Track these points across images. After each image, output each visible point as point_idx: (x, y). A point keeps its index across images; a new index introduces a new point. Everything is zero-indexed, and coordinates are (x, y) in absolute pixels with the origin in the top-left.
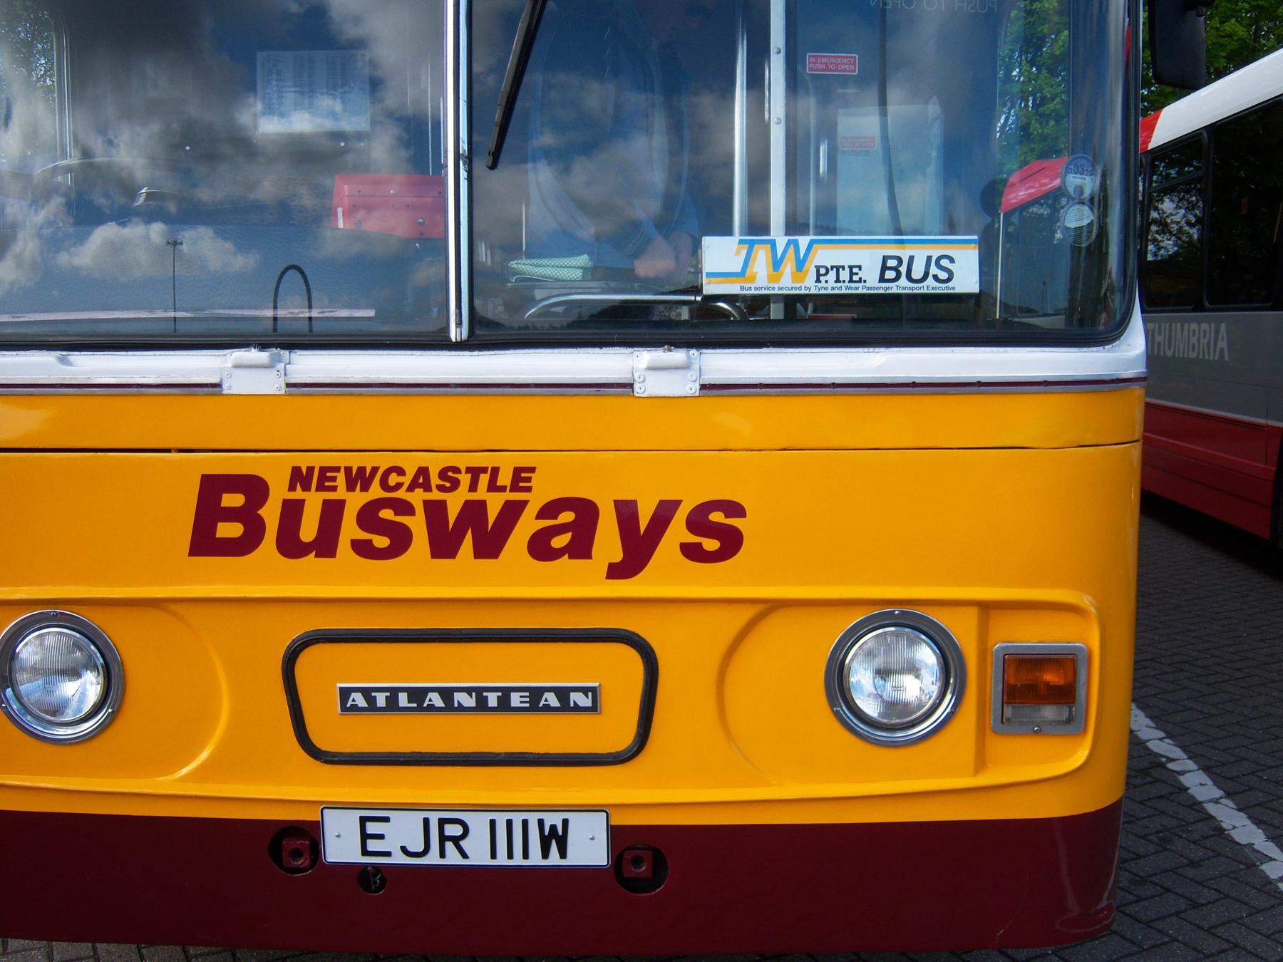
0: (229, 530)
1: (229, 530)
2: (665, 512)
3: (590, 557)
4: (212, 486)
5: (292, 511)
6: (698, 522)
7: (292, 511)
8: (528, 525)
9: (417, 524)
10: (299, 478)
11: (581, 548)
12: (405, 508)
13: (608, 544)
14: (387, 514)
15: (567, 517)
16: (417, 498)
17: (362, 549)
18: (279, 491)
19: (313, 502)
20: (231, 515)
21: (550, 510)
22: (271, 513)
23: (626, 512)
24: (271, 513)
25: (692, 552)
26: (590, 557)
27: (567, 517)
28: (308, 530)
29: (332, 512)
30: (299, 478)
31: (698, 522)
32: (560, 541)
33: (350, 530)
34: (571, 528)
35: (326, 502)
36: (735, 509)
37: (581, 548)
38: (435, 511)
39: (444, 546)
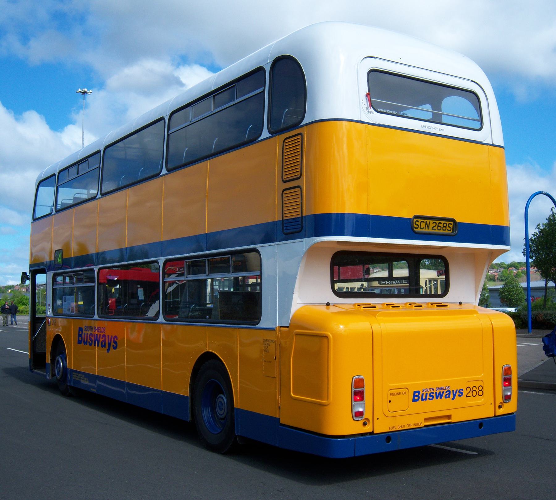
0: (416, 398)
1: (416, 398)
2: (457, 390)
4: (415, 392)
5: (423, 394)
7: (423, 394)
8: (445, 394)
9: (434, 395)
10: (424, 390)
11: (449, 397)
12: (433, 393)
13: (452, 396)
16: (434, 392)
17: (429, 399)
18: (421, 393)
19: (425, 393)
20: (417, 396)
22: (420, 395)
24: (420, 395)
25: (459, 395)
28: (424, 398)
29: (427, 394)
30: (424, 390)
31: (459, 392)
33: (428, 397)
36: (462, 390)
37: (449, 397)
38: (436, 393)
39: (437, 398)
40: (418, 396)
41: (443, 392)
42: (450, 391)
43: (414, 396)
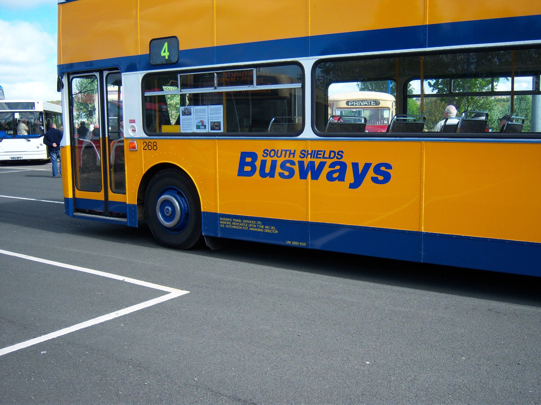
0: (247, 169)
1: (247, 169)
2: (367, 166)
3: (344, 181)
4: (244, 155)
5: (264, 163)
6: (377, 169)
7: (264, 163)
8: (326, 170)
9: (296, 168)
11: (341, 178)
12: (293, 163)
14: (288, 165)
15: (338, 167)
17: (281, 175)
18: (260, 158)
19: (269, 160)
20: (248, 164)
21: (332, 165)
22: (258, 164)
23: (355, 166)
24: (258, 164)
26: (344, 181)
27: (338, 167)
28: (267, 170)
29: (274, 163)
31: (377, 169)
32: (335, 175)
33: (278, 170)
34: (338, 172)
35: (272, 161)
36: (389, 166)
37: (341, 178)
38: (301, 164)
39: (303, 176)
40: (252, 165)
41: (322, 165)
42: (344, 166)
43: (242, 163)
